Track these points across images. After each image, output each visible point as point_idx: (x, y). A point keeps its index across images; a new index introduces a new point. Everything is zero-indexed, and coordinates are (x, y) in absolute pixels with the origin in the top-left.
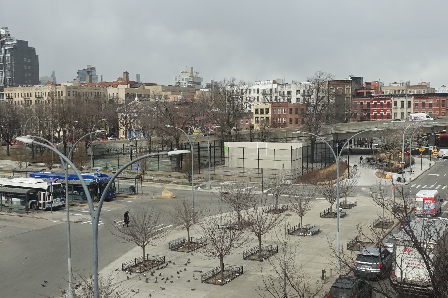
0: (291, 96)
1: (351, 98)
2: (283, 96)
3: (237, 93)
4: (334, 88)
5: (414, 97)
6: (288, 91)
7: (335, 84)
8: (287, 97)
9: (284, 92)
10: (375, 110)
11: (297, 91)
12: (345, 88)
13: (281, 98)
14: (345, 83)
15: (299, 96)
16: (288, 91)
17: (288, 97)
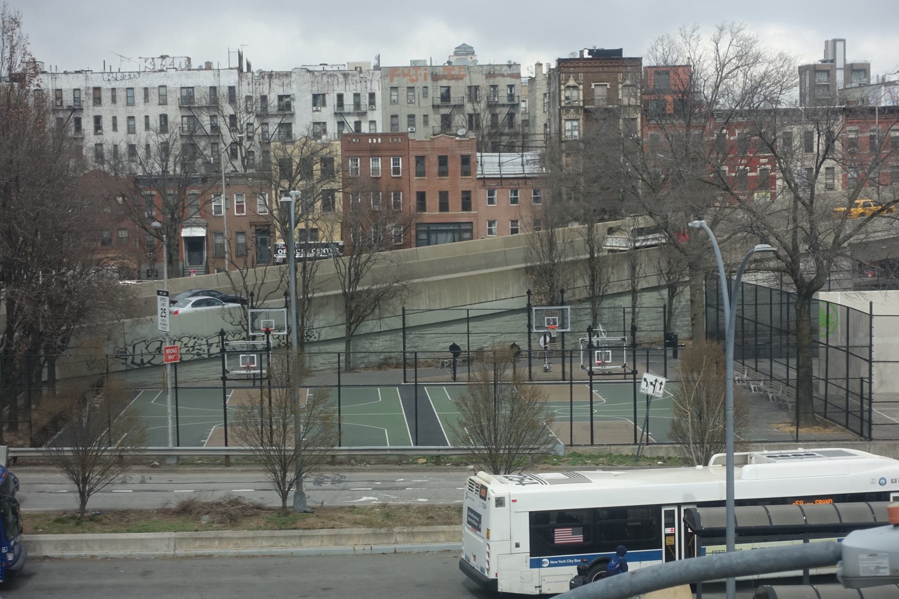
0: (292, 115)
1: (639, 120)
2: (263, 115)
3: (77, 99)
4: (581, 87)
5: (847, 116)
6: (281, 98)
7: (585, 69)
8: (275, 116)
9: (264, 98)
10: (762, 161)
11: (315, 97)
12: (620, 86)
13: (252, 119)
14: (616, 69)
15: (327, 114)
16: (281, 98)
17: (285, 115)
